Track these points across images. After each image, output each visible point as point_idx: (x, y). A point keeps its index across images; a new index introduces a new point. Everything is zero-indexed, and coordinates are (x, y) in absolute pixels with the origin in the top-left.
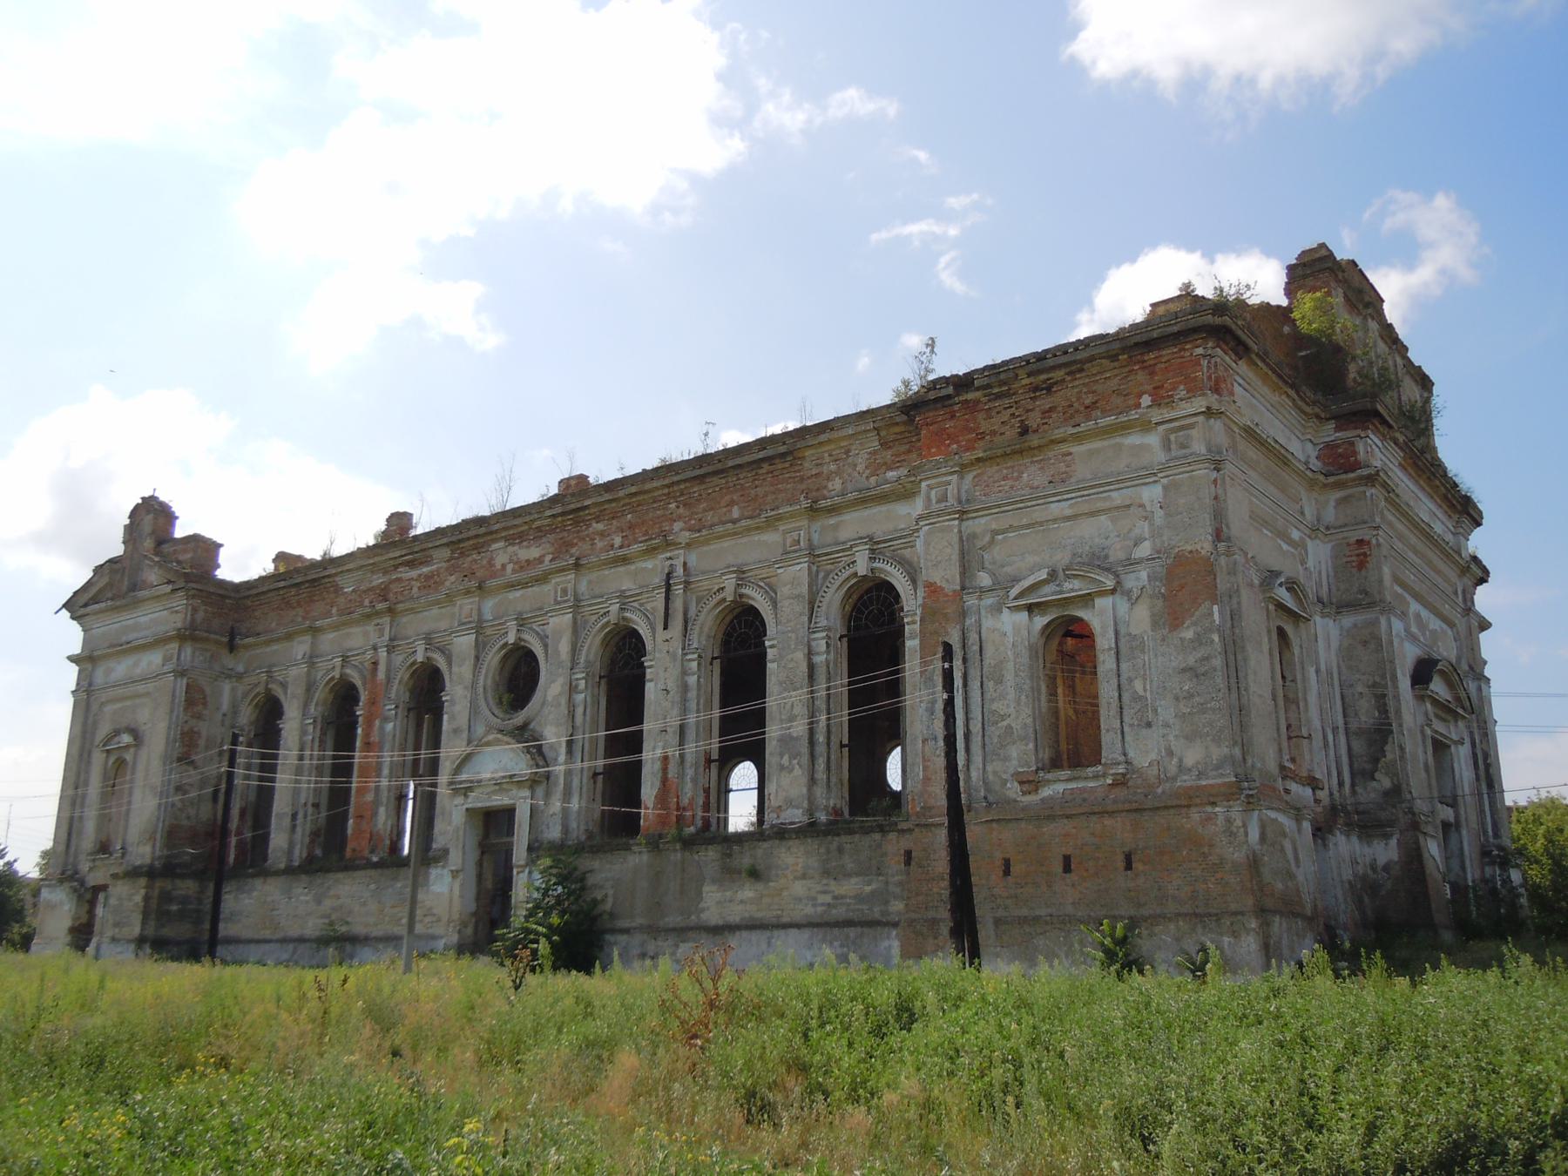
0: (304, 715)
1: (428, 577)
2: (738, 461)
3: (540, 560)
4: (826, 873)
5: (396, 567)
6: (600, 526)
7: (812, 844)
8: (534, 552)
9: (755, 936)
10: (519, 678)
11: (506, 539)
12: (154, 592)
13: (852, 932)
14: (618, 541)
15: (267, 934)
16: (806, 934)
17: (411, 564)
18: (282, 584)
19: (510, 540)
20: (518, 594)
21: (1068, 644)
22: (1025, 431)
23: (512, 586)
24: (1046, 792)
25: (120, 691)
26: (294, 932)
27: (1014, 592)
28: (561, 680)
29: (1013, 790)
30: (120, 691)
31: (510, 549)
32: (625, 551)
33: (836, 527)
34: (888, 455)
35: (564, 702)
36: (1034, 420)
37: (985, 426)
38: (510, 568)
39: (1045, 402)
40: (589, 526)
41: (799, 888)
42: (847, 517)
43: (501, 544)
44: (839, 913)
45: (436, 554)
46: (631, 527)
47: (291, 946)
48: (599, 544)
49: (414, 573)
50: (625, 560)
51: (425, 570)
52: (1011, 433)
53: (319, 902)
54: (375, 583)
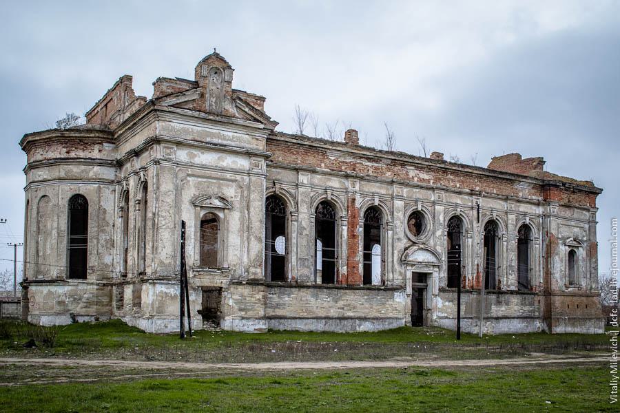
1: (376, 168)
2: (503, 176)
3: (429, 181)
4: (522, 304)
5: (361, 158)
6: (452, 177)
7: (518, 296)
8: (426, 176)
9: (507, 320)
11: (415, 166)
13: (529, 320)
15: (305, 315)
16: (518, 320)
17: (369, 159)
18: (295, 141)
20: (417, 190)
21: (572, 254)
22: (569, 201)
23: (417, 187)
24: (569, 290)
25: (208, 173)
26: (322, 313)
27: (568, 241)
28: (441, 230)
29: (564, 289)
30: (208, 173)
31: (416, 171)
33: (519, 206)
34: (533, 191)
35: (437, 237)
36: (571, 200)
37: (562, 196)
38: (416, 179)
39: (573, 196)
41: (516, 308)
42: (522, 204)
43: (413, 168)
44: (525, 315)
45: (384, 160)
47: (324, 321)
49: (370, 164)
50: (460, 193)
52: (567, 201)
53: (336, 302)
54: (347, 160)
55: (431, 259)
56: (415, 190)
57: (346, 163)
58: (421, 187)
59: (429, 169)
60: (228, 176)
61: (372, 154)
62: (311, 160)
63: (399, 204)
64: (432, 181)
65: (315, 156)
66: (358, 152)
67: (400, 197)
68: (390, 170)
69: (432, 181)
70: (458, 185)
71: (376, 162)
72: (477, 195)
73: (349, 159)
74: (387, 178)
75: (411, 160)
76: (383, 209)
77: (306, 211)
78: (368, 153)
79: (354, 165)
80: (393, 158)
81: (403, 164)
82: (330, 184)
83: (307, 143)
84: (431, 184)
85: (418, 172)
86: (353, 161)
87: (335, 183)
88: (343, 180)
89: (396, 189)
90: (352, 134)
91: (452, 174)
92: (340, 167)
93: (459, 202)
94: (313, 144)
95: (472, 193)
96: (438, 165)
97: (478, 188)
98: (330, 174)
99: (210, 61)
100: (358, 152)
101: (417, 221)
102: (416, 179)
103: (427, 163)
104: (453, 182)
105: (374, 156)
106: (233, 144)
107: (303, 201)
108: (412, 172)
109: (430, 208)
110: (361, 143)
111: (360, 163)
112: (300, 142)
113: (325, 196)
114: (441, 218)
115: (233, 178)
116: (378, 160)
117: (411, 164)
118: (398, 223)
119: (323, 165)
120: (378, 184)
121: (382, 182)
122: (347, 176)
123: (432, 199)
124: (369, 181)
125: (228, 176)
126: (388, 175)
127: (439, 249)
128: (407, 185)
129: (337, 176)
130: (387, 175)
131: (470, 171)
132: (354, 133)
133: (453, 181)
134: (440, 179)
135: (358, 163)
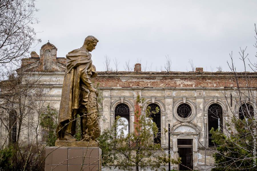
0: (111, 111)
1: (153, 83)
3: (192, 85)
5: (142, 78)
6: (210, 81)
8: (189, 83)
10: (184, 110)
12: (60, 73)
14: (215, 85)
19: (182, 79)
20: (184, 92)
28: (201, 113)
31: (182, 81)
32: (217, 88)
35: (200, 117)
38: (182, 85)
40: (206, 80)
43: (179, 79)
46: (218, 83)
48: (210, 85)
51: (152, 81)
55: (193, 131)
56: (182, 92)
57: (133, 82)
58: (186, 90)
59: (191, 79)
60: (55, 98)
61: (148, 76)
62: (111, 83)
63: (169, 101)
64: (194, 85)
65: (113, 82)
66: (139, 76)
67: (169, 97)
68: (163, 82)
69: (194, 85)
70: (215, 85)
71: (153, 79)
72: (230, 90)
73: (135, 80)
74: (161, 87)
75: (175, 76)
76: (158, 104)
77: (107, 110)
78: (146, 76)
79: (139, 83)
80: (163, 76)
81: (172, 78)
82: (123, 94)
83: (107, 76)
84: (194, 87)
85: (183, 81)
86: (138, 80)
87: (127, 93)
88: (132, 92)
89: (167, 93)
90: (138, 66)
91: (209, 79)
92: (129, 85)
93: (217, 95)
94: (111, 76)
95: (226, 89)
96: (197, 76)
97: (232, 85)
98: (123, 90)
99: (45, 47)
100: (139, 76)
101: (184, 110)
102: (182, 85)
103: (188, 76)
104: (210, 84)
105: (151, 76)
106: (58, 83)
107: (106, 105)
108: (179, 82)
109: (194, 101)
110: (143, 70)
111: (142, 81)
112: (102, 76)
113: (120, 101)
114: (201, 106)
115: (58, 99)
116: (154, 78)
117: (177, 77)
118: (168, 112)
119: (118, 85)
120: (156, 91)
121: (158, 90)
122: (133, 90)
123: (195, 96)
124: (148, 90)
125: (55, 98)
126: (162, 85)
127: (199, 124)
128: (174, 90)
129: (128, 90)
130: (161, 85)
131: (222, 76)
132: (138, 66)
133: (210, 83)
134: (200, 83)
135: (141, 81)
